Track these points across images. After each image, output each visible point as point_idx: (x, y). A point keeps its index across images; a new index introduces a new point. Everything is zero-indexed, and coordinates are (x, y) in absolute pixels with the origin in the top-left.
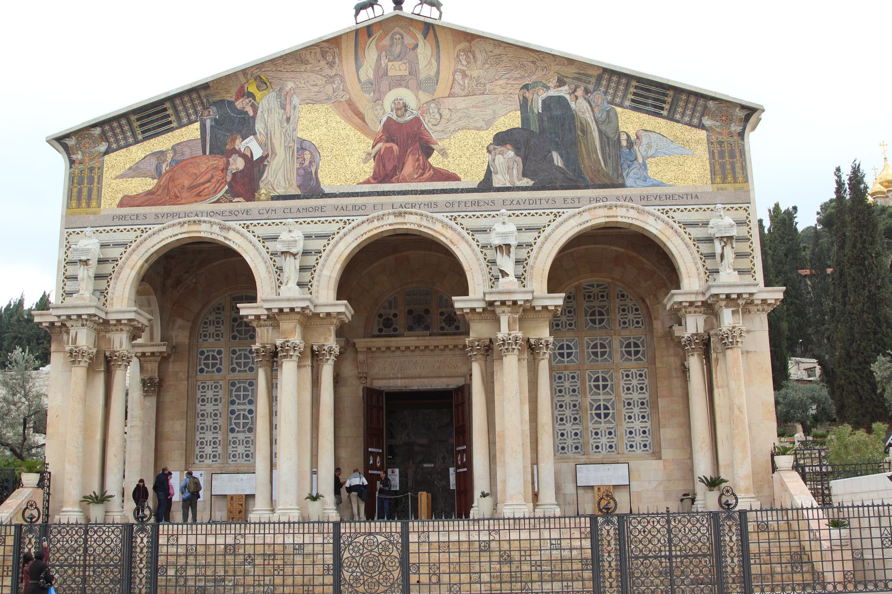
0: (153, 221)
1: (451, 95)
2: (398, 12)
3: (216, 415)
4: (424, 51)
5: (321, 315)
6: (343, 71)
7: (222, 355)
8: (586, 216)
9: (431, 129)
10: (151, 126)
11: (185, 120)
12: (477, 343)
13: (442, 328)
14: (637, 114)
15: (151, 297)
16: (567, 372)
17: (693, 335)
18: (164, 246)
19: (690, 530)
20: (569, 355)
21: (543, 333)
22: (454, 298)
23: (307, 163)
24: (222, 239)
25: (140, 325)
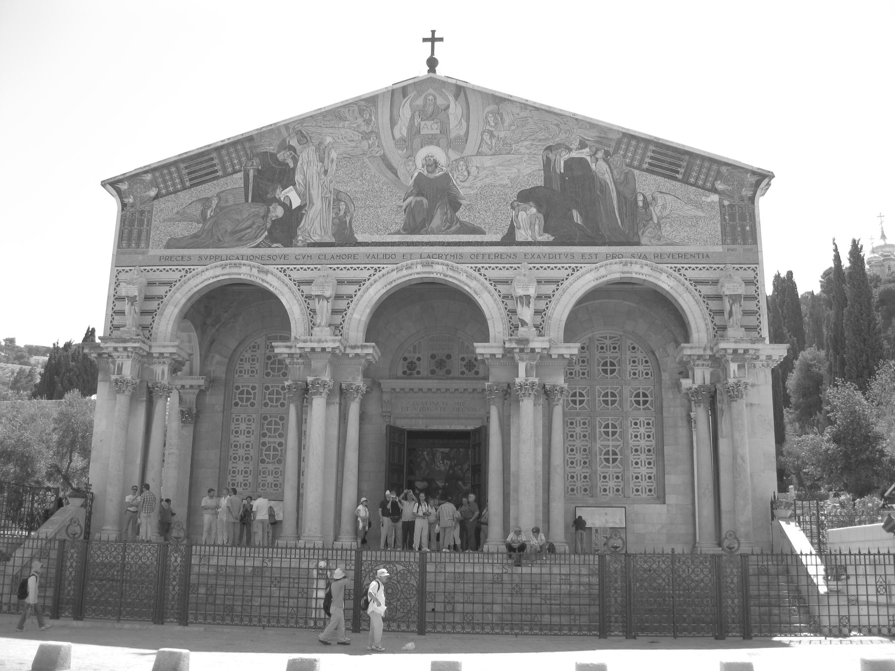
0: (196, 262)
1: (479, 154)
2: (431, 75)
3: (248, 446)
4: (455, 110)
5: (350, 356)
6: (378, 128)
7: (256, 391)
8: (602, 271)
9: (459, 185)
10: (198, 174)
11: (230, 170)
12: (495, 388)
13: (463, 373)
14: (655, 177)
15: (192, 333)
16: (578, 418)
17: (700, 386)
18: (206, 286)
19: (693, 571)
20: (581, 402)
22: (475, 344)
23: (342, 213)
24: (260, 282)
25: (180, 359)
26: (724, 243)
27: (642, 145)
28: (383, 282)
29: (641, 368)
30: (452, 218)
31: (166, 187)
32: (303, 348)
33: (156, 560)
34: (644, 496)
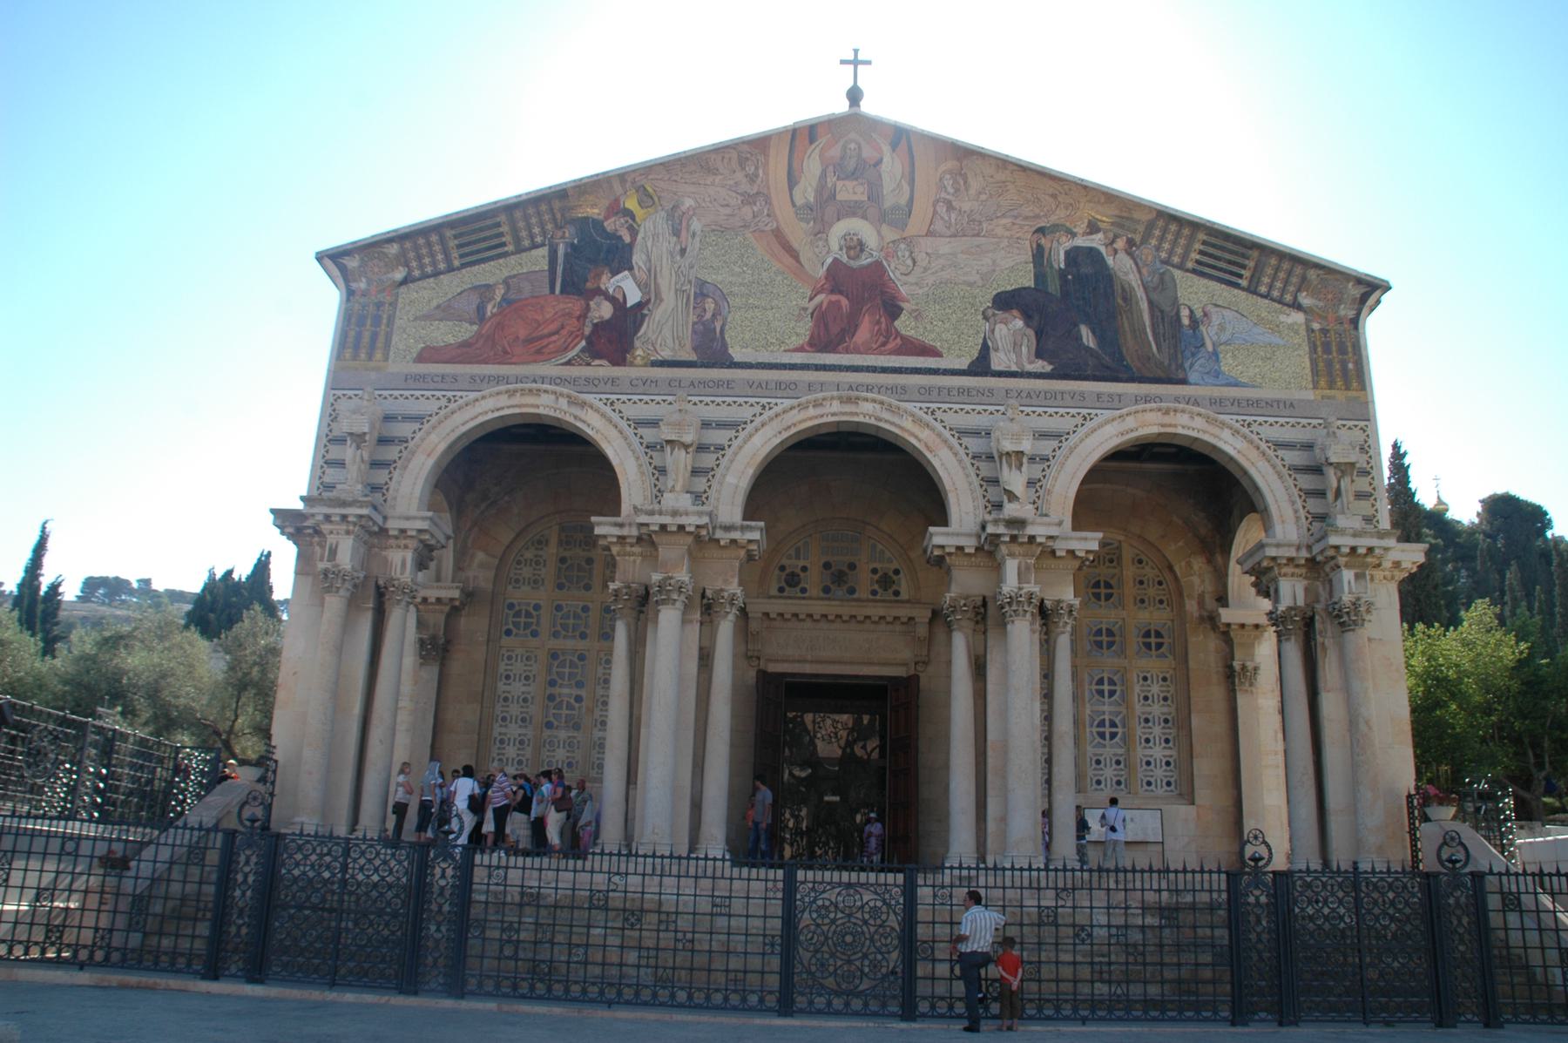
1: (930, 234)
2: (855, 110)
5: (722, 543)
6: (769, 188)
8: (1130, 422)
11: (526, 243)
12: (962, 602)
14: (1206, 281)
17: (1290, 609)
18: (482, 424)
21: (1066, 593)
22: (932, 529)
23: (708, 316)
24: (572, 420)
25: (433, 542)
26: (1315, 387)
27: (1186, 231)
28: (776, 425)
29: (1152, 591)
30: (887, 331)
31: (422, 267)
32: (647, 525)
33: (406, 873)
34: (1160, 792)
